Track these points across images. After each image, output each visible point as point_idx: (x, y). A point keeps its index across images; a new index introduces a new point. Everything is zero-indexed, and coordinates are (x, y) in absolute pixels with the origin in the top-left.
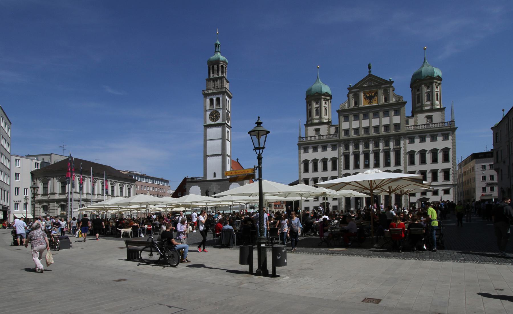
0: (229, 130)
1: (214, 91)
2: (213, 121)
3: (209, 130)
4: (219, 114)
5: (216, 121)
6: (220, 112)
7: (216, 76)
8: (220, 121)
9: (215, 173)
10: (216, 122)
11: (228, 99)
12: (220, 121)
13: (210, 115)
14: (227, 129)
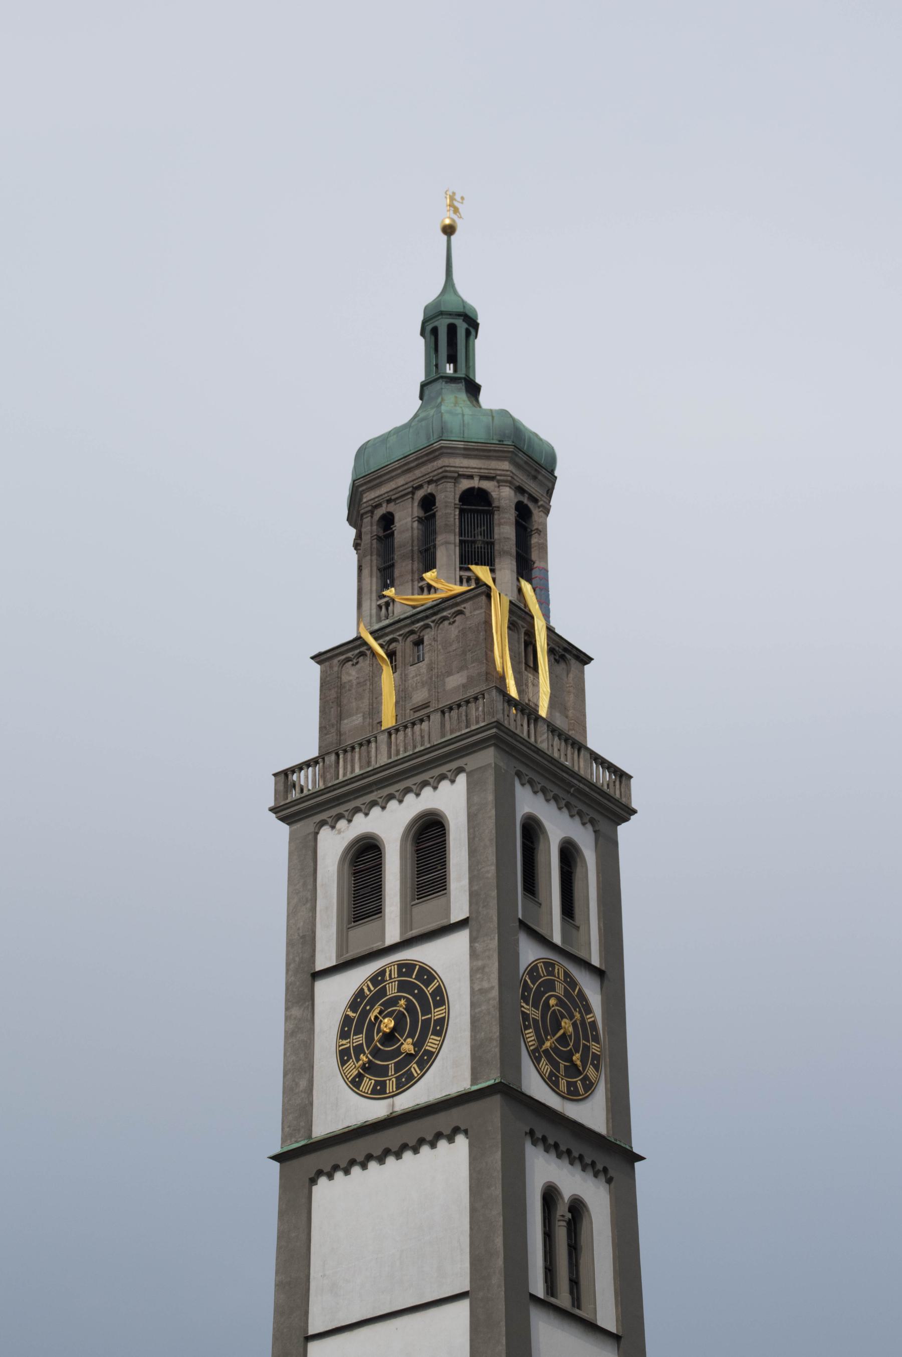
0: (573, 1182)
2: (379, 1092)
4: (440, 998)
5: (406, 1082)
6: (449, 959)
8: (449, 1072)
10: (406, 1101)
11: (558, 827)
12: (449, 1072)
13: (346, 1028)
14: (543, 1169)
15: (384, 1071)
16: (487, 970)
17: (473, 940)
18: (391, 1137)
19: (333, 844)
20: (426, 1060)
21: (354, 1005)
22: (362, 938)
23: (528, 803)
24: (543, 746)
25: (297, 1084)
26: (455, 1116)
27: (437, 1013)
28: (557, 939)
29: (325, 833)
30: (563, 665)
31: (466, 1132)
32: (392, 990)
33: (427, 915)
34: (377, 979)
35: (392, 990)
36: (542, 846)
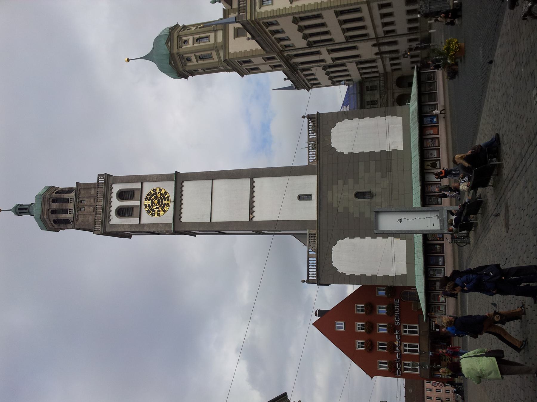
1: (100, 203)
2: (168, 205)
3: (187, 217)
5: (168, 199)
6: (148, 188)
7: (71, 205)
9: (300, 197)
10: (172, 198)
13: (153, 215)
15: (165, 204)
18: (178, 201)
19: (115, 220)
20: (166, 193)
21: (149, 212)
22: (136, 212)
26: (179, 184)
27: (158, 190)
29: (111, 223)
31: (183, 182)
32: (149, 202)
33: (137, 194)
34: (146, 207)
35: (149, 202)
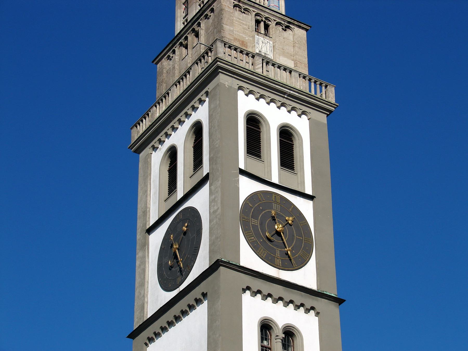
6: (200, 202)
11: (275, 116)
16: (216, 199)
17: (210, 186)
23: (246, 103)
24: (259, 71)
25: (140, 294)
28: (275, 180)
30: (289, 31)
36: (263, 130)
